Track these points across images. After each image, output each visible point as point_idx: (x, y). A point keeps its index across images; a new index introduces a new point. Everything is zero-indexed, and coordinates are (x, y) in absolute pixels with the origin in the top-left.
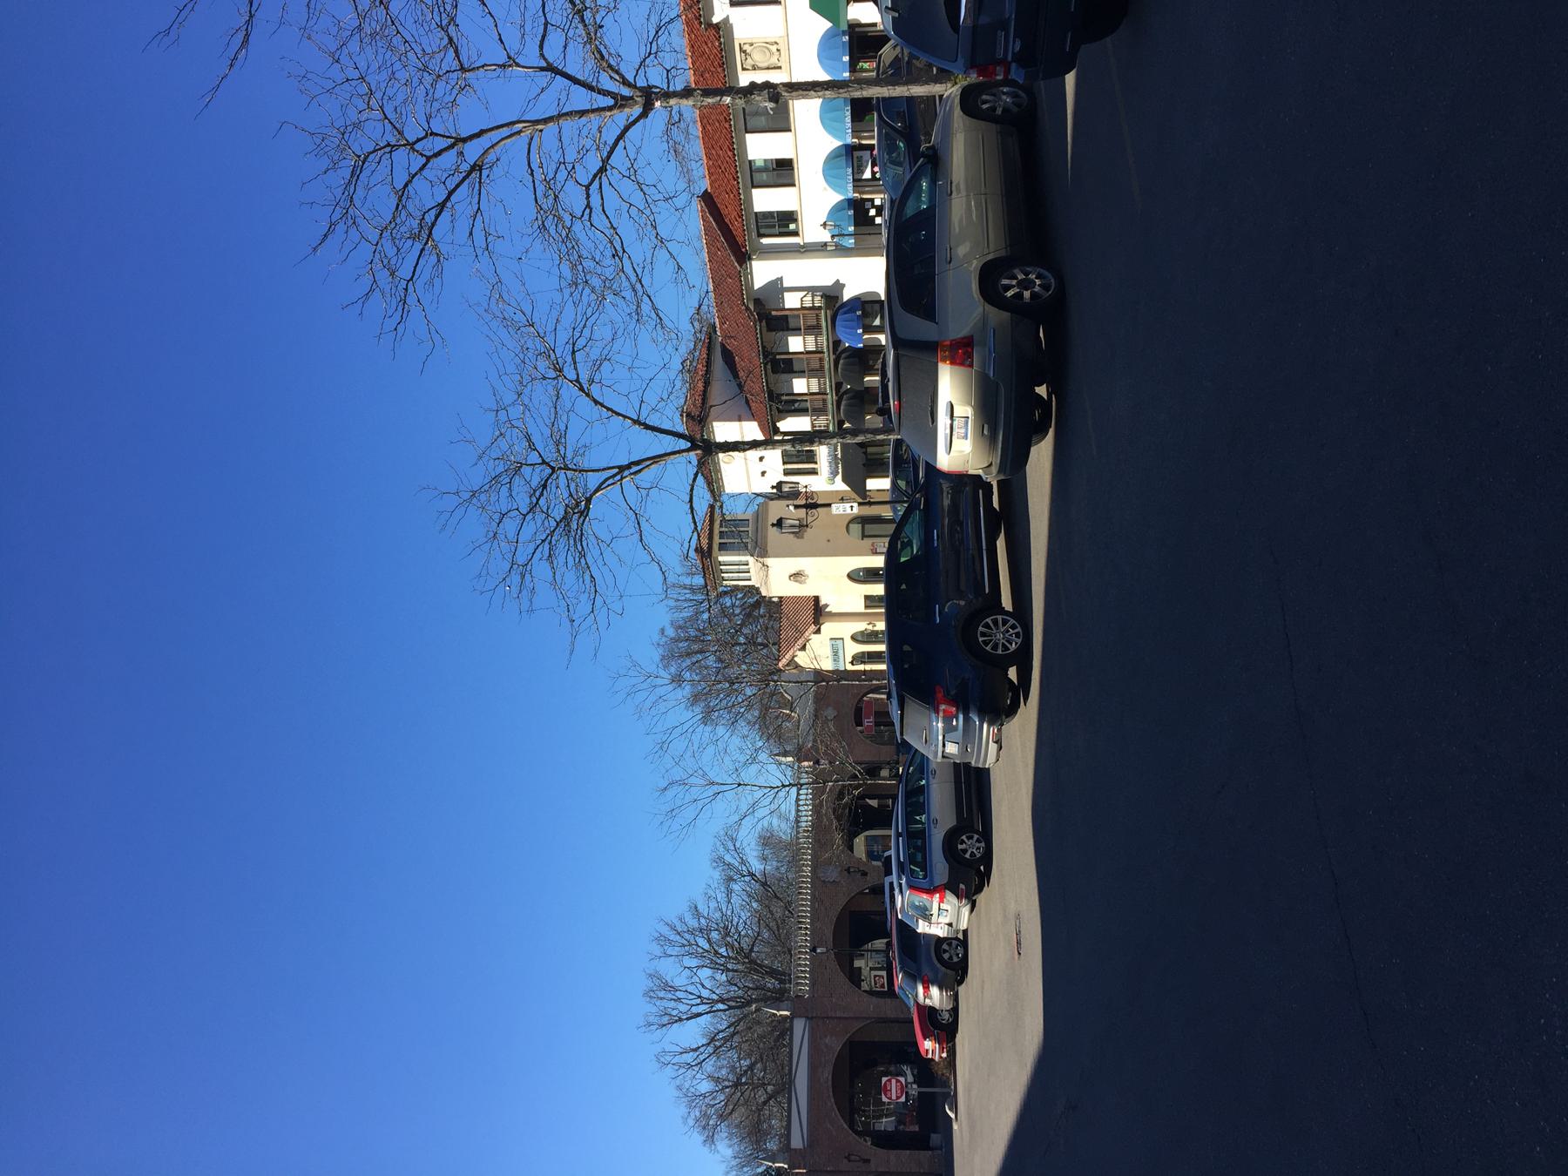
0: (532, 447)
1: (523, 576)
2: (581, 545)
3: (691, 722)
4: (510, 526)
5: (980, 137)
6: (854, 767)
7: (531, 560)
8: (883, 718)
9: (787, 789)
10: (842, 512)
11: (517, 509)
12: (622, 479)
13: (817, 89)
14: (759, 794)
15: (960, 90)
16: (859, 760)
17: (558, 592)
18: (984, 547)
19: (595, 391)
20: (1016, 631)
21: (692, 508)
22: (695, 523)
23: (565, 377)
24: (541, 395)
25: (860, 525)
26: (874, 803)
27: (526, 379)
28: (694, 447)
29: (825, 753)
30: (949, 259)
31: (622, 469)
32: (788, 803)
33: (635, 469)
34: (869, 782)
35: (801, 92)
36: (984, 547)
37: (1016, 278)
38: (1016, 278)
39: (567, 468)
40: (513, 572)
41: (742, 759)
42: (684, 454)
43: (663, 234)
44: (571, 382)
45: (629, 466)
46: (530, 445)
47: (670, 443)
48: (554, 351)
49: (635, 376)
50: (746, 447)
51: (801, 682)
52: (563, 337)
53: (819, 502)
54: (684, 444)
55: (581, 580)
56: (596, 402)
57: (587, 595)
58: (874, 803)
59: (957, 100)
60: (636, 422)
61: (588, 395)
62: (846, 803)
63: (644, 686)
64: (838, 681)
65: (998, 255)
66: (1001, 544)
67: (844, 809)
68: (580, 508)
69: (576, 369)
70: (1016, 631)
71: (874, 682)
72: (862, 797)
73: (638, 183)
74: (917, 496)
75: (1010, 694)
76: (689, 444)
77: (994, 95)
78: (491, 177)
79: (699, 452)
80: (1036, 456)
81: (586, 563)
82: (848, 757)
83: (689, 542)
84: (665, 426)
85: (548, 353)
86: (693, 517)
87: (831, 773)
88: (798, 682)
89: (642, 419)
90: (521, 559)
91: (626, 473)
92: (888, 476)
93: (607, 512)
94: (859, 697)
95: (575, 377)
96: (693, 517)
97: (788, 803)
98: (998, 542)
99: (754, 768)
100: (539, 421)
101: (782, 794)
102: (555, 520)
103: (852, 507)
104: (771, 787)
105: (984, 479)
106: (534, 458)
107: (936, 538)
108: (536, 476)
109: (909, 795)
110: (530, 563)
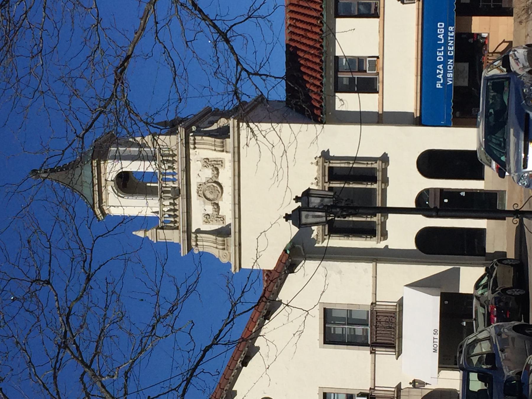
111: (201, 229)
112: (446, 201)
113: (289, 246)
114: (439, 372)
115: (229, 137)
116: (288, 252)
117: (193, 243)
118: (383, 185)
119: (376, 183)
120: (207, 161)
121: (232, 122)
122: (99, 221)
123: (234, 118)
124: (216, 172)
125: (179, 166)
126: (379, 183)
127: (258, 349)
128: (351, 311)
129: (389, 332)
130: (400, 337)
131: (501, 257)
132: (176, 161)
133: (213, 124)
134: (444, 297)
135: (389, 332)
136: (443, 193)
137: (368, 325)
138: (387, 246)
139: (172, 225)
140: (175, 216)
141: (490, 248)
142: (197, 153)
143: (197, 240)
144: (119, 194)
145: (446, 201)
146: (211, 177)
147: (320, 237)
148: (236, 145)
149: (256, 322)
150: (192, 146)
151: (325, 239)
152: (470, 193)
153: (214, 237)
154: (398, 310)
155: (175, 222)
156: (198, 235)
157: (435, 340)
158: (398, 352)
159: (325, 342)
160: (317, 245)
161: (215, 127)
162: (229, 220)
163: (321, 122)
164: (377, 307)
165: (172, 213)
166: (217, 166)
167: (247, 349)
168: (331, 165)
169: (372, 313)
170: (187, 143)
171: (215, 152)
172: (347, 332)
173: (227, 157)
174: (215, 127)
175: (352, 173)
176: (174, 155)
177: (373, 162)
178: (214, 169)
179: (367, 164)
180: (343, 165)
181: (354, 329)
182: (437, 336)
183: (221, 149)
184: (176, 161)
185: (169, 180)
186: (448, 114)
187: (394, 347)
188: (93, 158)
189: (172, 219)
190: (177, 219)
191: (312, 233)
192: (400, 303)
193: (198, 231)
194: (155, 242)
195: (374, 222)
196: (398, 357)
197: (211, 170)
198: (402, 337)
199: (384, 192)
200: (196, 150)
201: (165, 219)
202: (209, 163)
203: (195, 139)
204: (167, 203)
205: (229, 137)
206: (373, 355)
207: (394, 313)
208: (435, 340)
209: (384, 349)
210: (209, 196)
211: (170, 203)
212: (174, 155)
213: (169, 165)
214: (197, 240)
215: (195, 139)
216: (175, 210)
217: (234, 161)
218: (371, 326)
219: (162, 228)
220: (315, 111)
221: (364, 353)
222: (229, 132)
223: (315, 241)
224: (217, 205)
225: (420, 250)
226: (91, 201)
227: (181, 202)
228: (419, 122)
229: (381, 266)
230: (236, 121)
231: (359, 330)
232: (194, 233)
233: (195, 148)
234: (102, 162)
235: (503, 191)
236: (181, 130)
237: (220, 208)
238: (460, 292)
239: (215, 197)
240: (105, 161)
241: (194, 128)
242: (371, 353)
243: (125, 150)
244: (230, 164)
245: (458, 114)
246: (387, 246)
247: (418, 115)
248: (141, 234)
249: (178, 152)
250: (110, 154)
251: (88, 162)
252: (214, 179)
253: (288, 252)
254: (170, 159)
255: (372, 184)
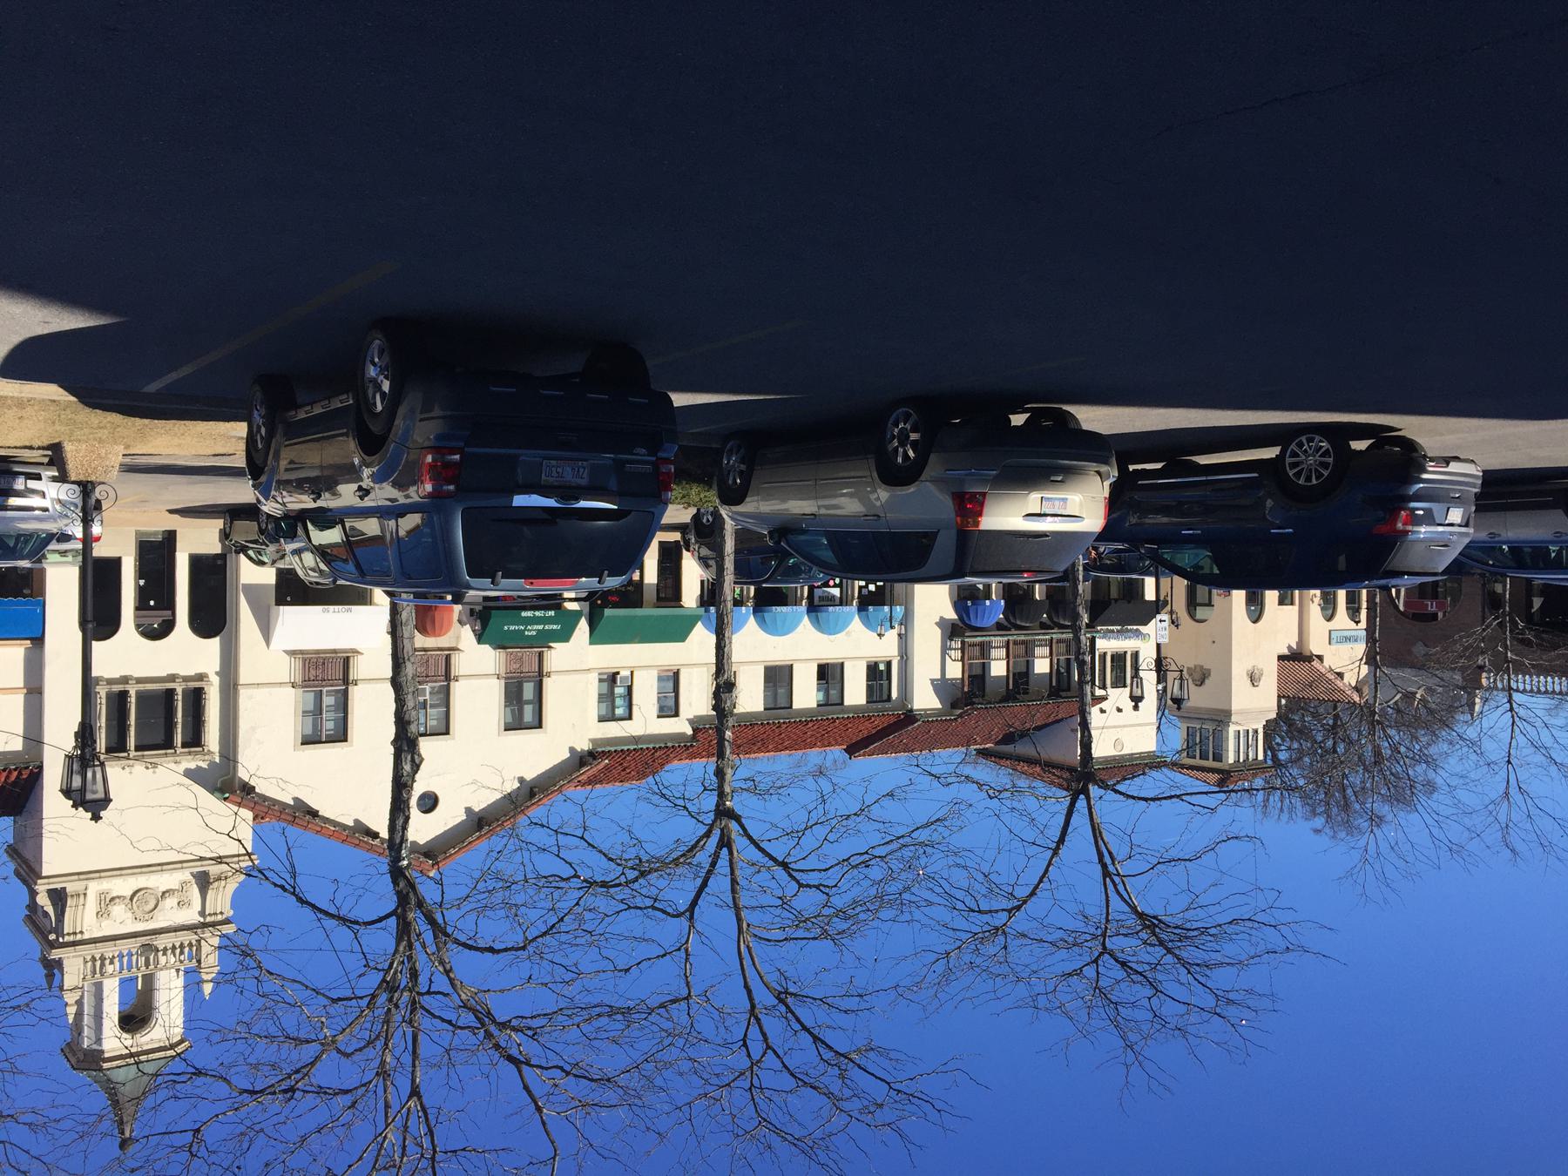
0: (1078, 972)
1: (1230, 1002)
2: (1193, 930)
3: (1426, 816)
4: (1169, 1009)
5: (766, 485)
6: (1487, 627)
7: (1210, 989)
8: (1423, 592)
9: (1515, 705)
10: (1167, 632)
11: (1150, 998)
12: (1118, 875)
13: (723, 645)
14: (1521, 740)
15: (724, 506)
16: (1480, 619)
17: (1252, 961)
18: (1204, 478)
19: (1022, 892)
20: (1305, 441)
21: (1153, 799)
22: (1171, 797)
23: (1004, 925)
24: (1022, 954)
25: (1198, 608)
26: (1537, 603)
27: (1005, 969)
28: (1086, 792)
29: (1469, 658)
30: (875, 518)
31: (1106, 873)
32: (1535, 705)
33: (1107, 860)
34: (1507, 609)
35: (725, 661)
36: (1204, 478)
37: (896, 450)
38: (897, 447)
39: (1104, 935)
40: (1224, 1013)
41: (1473, 757)
42: (1092, 803)
43: (855, 808)
44: (1010, 918)
45: (1104, 866)
46: (1075, 975)
47: (1080, 820)
48: (976, 934)
49: (1007, 848)
50: (1086, 734)
51: (1376, 683)
52: (960, 923)
53: (1155, 657)
54: (1081, 803)
55: (1233, 937)
56: (1033, 893)
57: (1253, 932)
58: (1537, 603)
59: (734, 508)
60: (1056, 852)
61: (1025, 902)
62: (1535, 637)
63: (1378, 866)
64: (1375, 641)
65: (873, 468)
66: (1203, 460)
67: (1543, 639)
68: (1150, 923)
69: (997, 911)
70: (1305, 441)
71: (1378, 600)
72: (1529, 619)
73: (806, 829)
74: (1143, 551)
75: (1387, 447)
76: (1082, 796)
77: (729, 471)
78: (796, 980)
79: (1090, 786)
80: (1095, 423)
81: (1215, 927)
82: (1475, 632)
83: (1194, 805)
84: (1061, 819)
85: (980, 938)
86: (1165, 798)
87: (1496, 654)
88: (1376, 687)
89: (1054, 846)
90: (1209, 1002)
91: (1111, 868)
92: (1143, 579)
93: (1156, 897)
94: (1400, 616)
95: (1006, 913)
96: (1165, 798)
97: (1535, 705)
98: (1202, 463)
99: (1487, 745)
100: (1049, 961)
101: (1522, 712)
102: (1165, 955)
103: (1161, 621)
104: (1513, 725)
105: (1115, 479)
106: (1090, 971)
107: (1191, 532)
108: (1112, 971)
109: (1521, 566)
110: (1215, 991)
111: (200, 910)
112: (152, 603)
113: (217, 794)
114: (377, 605)
115: (65, 888)
116: (227, 795)
117: (219, 918)
118: (130, 682)
119: (128, 691)
120: (101, 913)
121: (42, 888)
122: (191, 1047)
123: (36, 884)
124: (117, 900)
125: (109, 950)
126: (128, 687)
127: (356, 821)
128: (304, 712)
129: (330, 665)
130: (335, 651)
131: (225, 535)
132: (102, 955)
133: (47, 912)
134: (281, 601)
135: (330, 665)
136: (141, 606)
137: (321, 691)
138: (217, 673)
139: (195, 948)
140: (182, 946)
141: (216, 549)
142: (89, 928)
143: (215, 914)
144: (152, 1026)
145: (152, 603)
146: (124, 906)
147: (206, 757)
148: (76, 877)
149: (322, 827)
150: (79, 937)
151: (209, 751)
152: (142, 572)
153: (210, 892)
154: (301, 656)
155: (190, 945)
156: (207, 913)
157: (336, 610)
158: (353, 652)
159: (345, 740)
160: (217, 760)
161: (50, 910)
162: (185, 875)
163: (41, 768)
164: (297, 681)
165: (178, 951)
166: (108, 900)
167: (357, 835)
168: (103, 751)
169: (306, 687)
170: (74, 944)
171: (87, 906)
172: (332, 715)
173: (94, 888)
174: (50, 910)
175: (115, 723)
176: (94, 959)
177: (98, 696)
178: (112, 903)
179: (100, 704)
180: (103, 736)
181: (327, 706)
182: (331, 608)
183: (82, 897)
184: (102, 955)
185: (130, 961)
186: (26, 604)
187: (348, 657)
188: (101, 1069)
189: (186, 950)
190: (186, 943)
191: (201, 767)
192: (292, 653)
193: (202, 913)
194: (219, 968)
195: (183, 691)
196: (358, 652)
197: (115, 907)
198: (335, 650)
199: (139, 681)
200: (84, 930)
201: (186, 958)
202: (103, 910)
203: (68, 934)
204: (163, 960)
205: (65, 888)
206: (358, 682)
207: (304, 660)
208: (336, 610)
209: (351, 670)
210: (152, 905)
211: (163, 955)
212: (94, 959)
213: (107, 962)
214: (215, 914)
215: (68, 934)
216: (174, 948)
217: (100, 877)
218: (323, 686)
219: (199, 961)
220: (25, 777)
221: (356, 693)
222: (57, 889)
223: (212, 764)
224: (164, 893)
225: (221, 632)
226: (163, 1062)
227: (162, 942)
228: (38, 641)
229: (242, 680)
230: (39, 881)
231: (328, 701)
232: (205, 920)
233: (81, 932)
234: (106, 1055)
235: (136, 534)
236: (55, 954)
237: (168, 888)
238: (274, 583)
239: (153, 897)
240: (102, 1052)
241: (52, 937)
242: (356, 685)
243: (88, 1027)
244: (104, 883)
245: (26, 591)
246: (217, 673)
247: (29, 642)
248: (208, 988)
249: (89, 954)
250: (95, 1047)
251: (105, 1075)
252: (127, 901)
253: (227, 795)
254: (98, 963)
255: (130, 697)
